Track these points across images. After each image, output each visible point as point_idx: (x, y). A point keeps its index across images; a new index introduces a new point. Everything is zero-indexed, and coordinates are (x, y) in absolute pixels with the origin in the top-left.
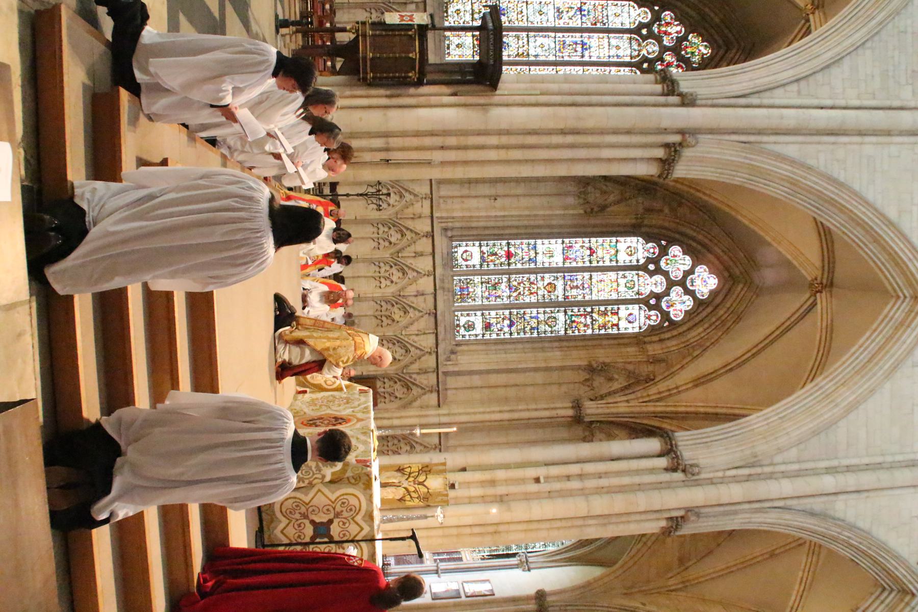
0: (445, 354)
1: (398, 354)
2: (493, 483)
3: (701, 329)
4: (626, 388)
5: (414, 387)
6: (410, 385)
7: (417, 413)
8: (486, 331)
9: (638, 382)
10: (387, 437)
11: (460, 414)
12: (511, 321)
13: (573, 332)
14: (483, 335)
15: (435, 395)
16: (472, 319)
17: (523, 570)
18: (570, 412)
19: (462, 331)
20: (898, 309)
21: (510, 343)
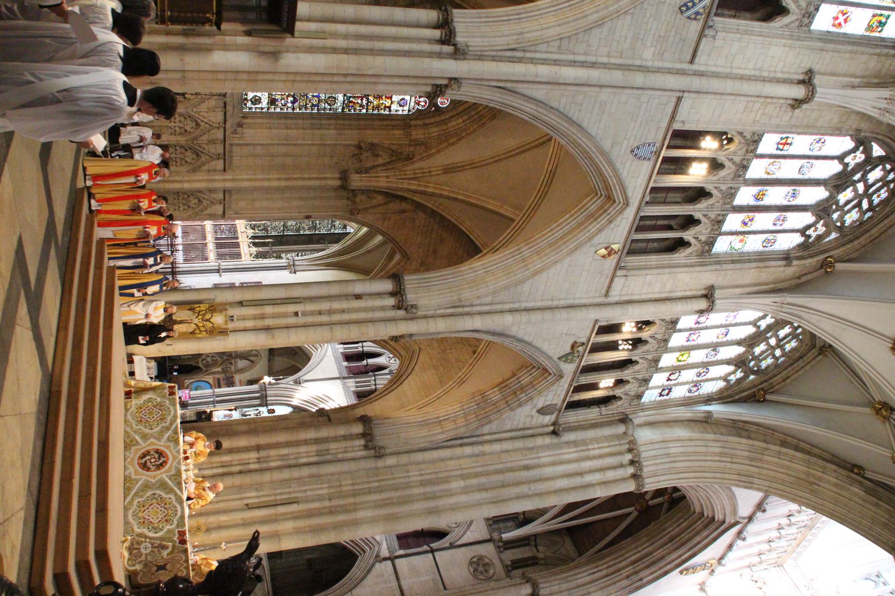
0: (232, 127)
1: (189, 126)
2: (262, 317)
3: (460, 120)
4: (388, 163)
5: (202, 155)
6: (200, 153)
7: (206, 177)
8: (271, 105)
9: (399, 160)
10: (178, 193)
11: (243, 180)
12: (295, 98)
13: (349, 110)
14: (268, 109)
15: (221, 162)
16: (259, 94)
17: (290, 273)
18: (338, 183)
19: (249, 104)
20: (594, 203)
21: (292, 118)
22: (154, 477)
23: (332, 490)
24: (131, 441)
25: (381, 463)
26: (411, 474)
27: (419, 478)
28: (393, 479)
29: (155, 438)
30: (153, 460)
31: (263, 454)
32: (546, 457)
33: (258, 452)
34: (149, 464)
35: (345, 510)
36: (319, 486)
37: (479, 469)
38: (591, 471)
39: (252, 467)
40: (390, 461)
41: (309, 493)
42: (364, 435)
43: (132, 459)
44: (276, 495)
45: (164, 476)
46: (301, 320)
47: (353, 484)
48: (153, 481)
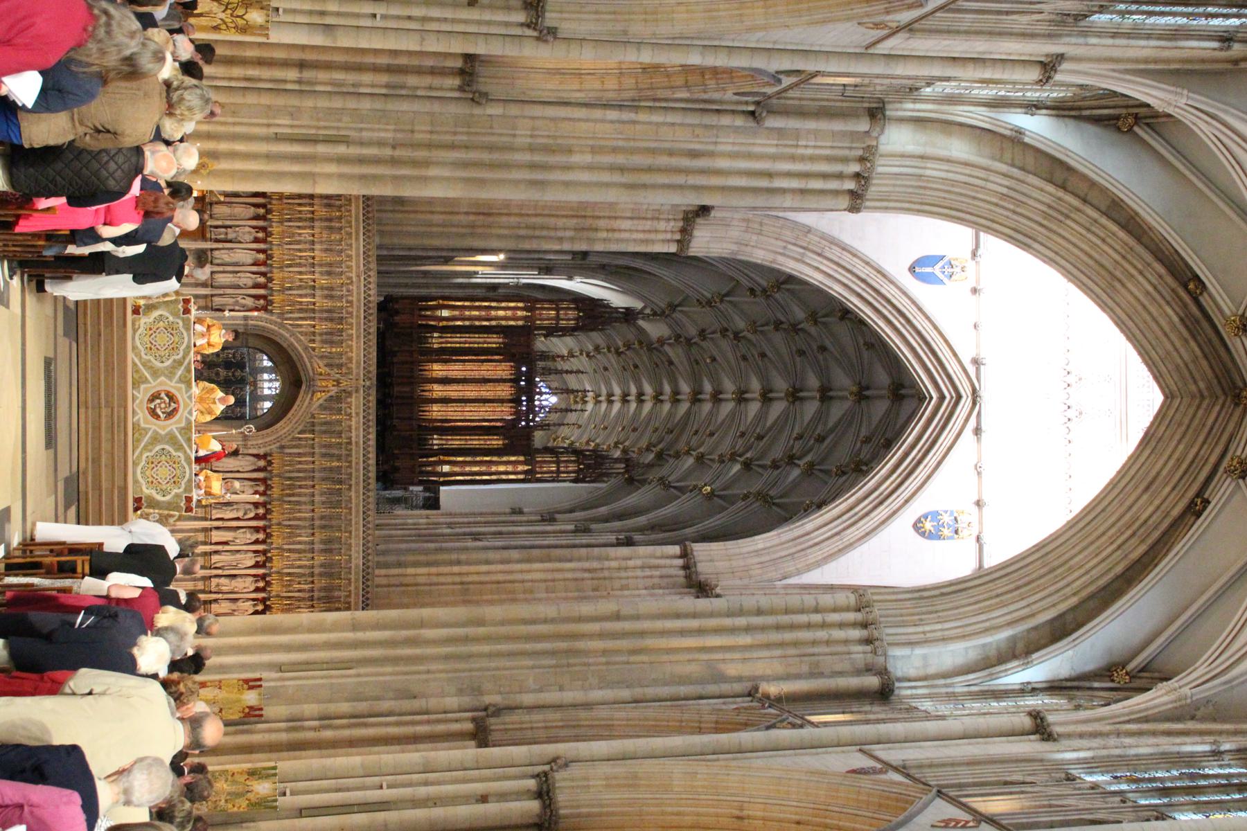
22: (164, 428)
23: (399, 135)
24: (140, 377)
25: (477, 111)
26: (517, 132)
27: (529, 140)
28: (493, 134)
29: (166, 376)
30: (163, 405)
31: (308, 74)
32: (727, 143)
33: (301, 72)
34: (158, 401)
35: (415, 163)
36: (381, 126)
37: (621, 143)
38: (789, 175)
39: (289, 87)
40: (494, 110)
41: (365, 134)
42: (462, 72)
43: (141, 402)
44: (318, 128)
45: (174, 427)
46: (379, 23)
47: (431, 132)
48: (163, 433)
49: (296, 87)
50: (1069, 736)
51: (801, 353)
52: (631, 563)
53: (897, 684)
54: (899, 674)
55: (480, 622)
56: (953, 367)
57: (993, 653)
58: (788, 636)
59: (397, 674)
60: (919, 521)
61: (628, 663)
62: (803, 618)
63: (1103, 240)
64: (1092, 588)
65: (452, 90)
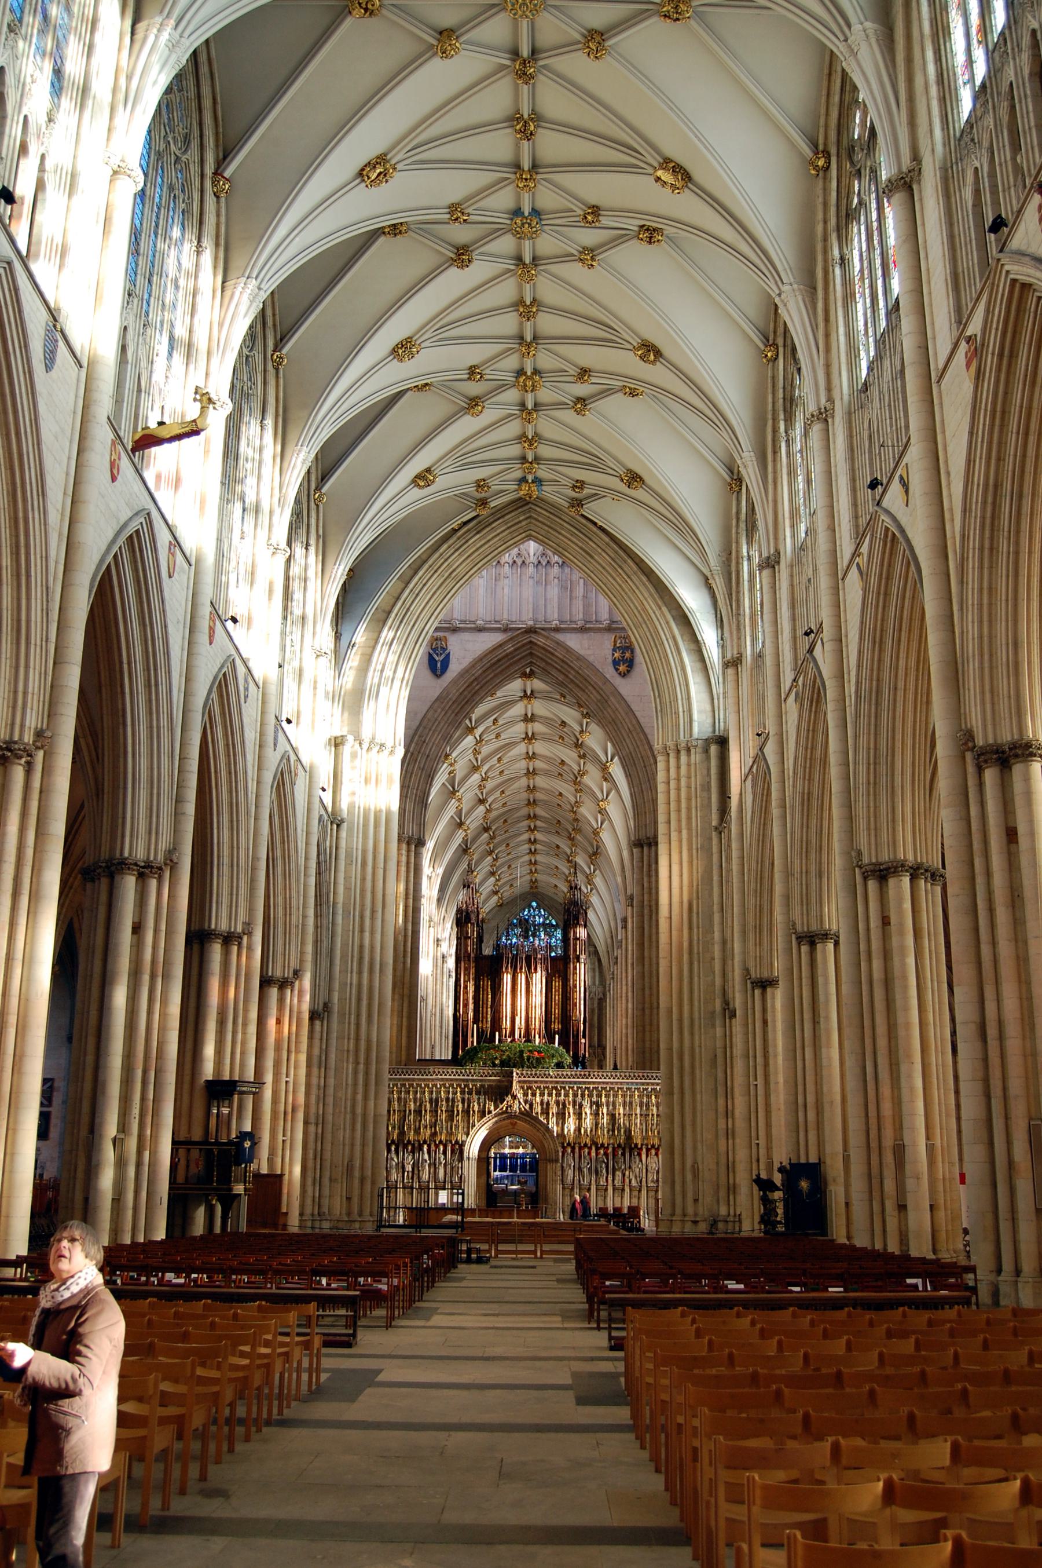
25: (336, 1008)
31: (312, 1119)
39: (320, 1131)
40: (336, 996)
47: (349, 1039)
49: (320, 1126)
50: (739, 646)
51: (498, 736)
52: (646, 885)
53: (717, 733)
54: (710, 730)
55: (670, 1011)
56: (509, 648)
57: (699, 665)
58: (684, 805)
59: (701, 1068)
60: (620, 674)
61: (698, 913)
62: (673, 793)
63: (425, 585)
64: (656, 596)
65: (322, 1025)
